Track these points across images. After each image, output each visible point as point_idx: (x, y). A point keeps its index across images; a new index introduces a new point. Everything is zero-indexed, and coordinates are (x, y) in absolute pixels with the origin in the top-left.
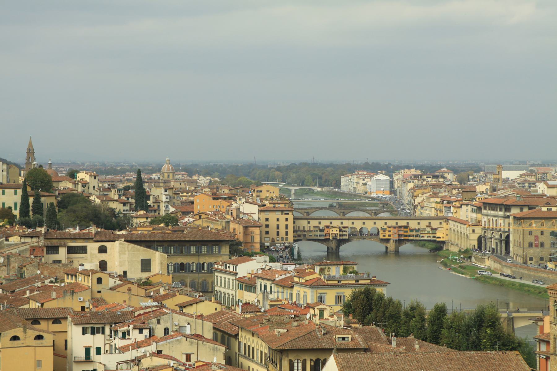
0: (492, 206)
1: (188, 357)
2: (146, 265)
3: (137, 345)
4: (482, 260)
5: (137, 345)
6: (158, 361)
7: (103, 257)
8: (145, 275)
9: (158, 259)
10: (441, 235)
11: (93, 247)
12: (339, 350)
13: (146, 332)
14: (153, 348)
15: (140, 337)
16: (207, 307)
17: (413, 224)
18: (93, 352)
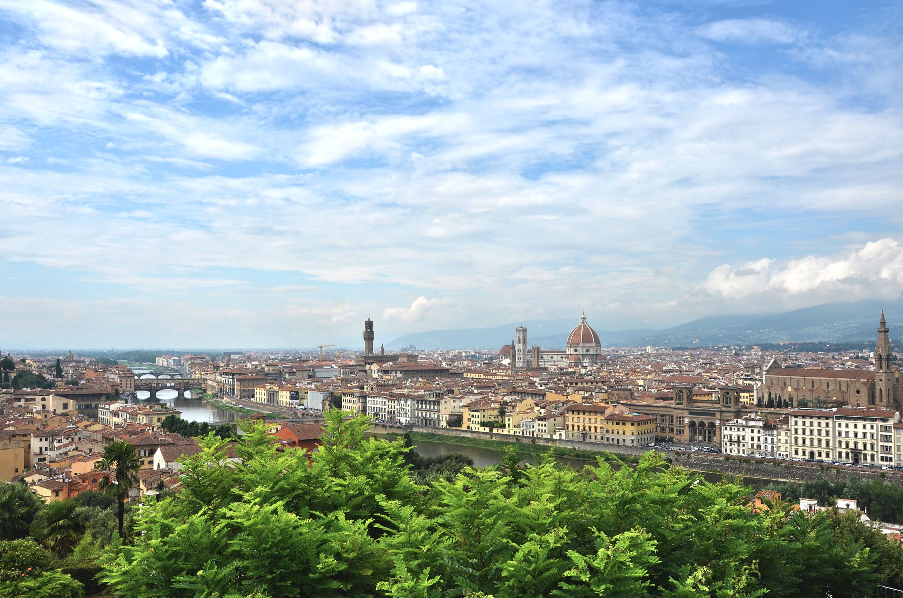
0: (227, 374)
1: (91, 450)
2: (65, 406)
3: (66, 446)
4: (222, 398)
5: (66, 446)
6: (76, 453)
7: (43, 403)
8: (65, 411)
9: (71, 403)
10: (203, 386)
11: (38, 399)
12: (161, 445)
13: (70, 440)
14: (74, 447)
15: (67, 442)
16: (98, 427)
17: (191, 382)
18: (43, 450)
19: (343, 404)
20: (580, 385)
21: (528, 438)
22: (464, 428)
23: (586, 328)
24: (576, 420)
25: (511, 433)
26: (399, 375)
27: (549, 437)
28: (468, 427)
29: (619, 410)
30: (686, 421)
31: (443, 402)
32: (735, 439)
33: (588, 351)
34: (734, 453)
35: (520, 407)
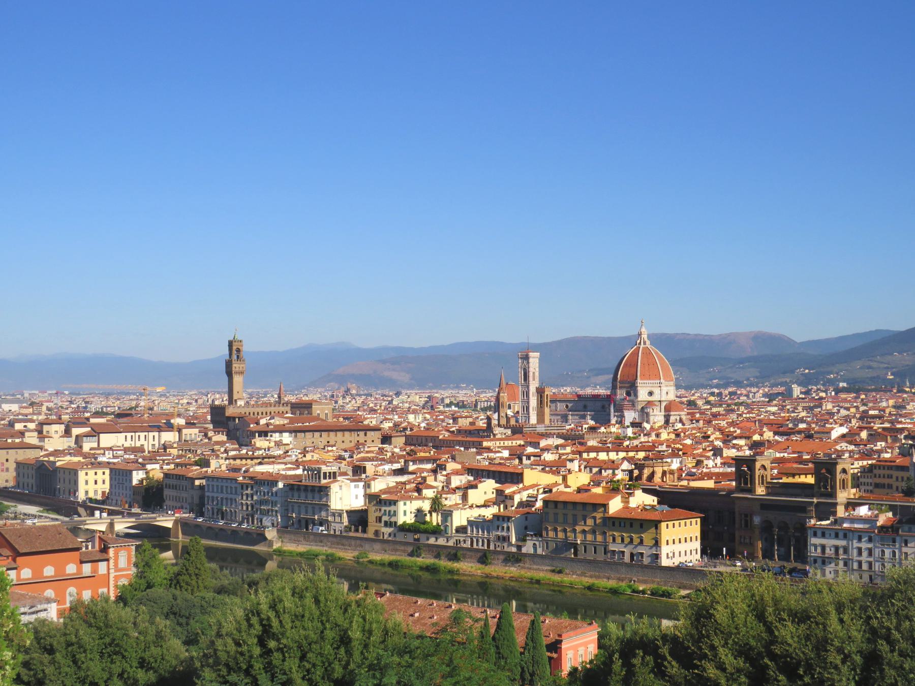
19: (167, 492)
20: (603, 456)
21: (478, 550)
22: (370, 534)
23: (647, 352)
24: (561, 519)
25: (451, 543)
26: (287, 438)
27: (514, 550)
28: (377, 533)
29: (641, 499)
30: (757, 520)
31: (334, 488)
32: (829, 552)
33: (651, 394)
34: (829, 576)
35: (475, 496)
